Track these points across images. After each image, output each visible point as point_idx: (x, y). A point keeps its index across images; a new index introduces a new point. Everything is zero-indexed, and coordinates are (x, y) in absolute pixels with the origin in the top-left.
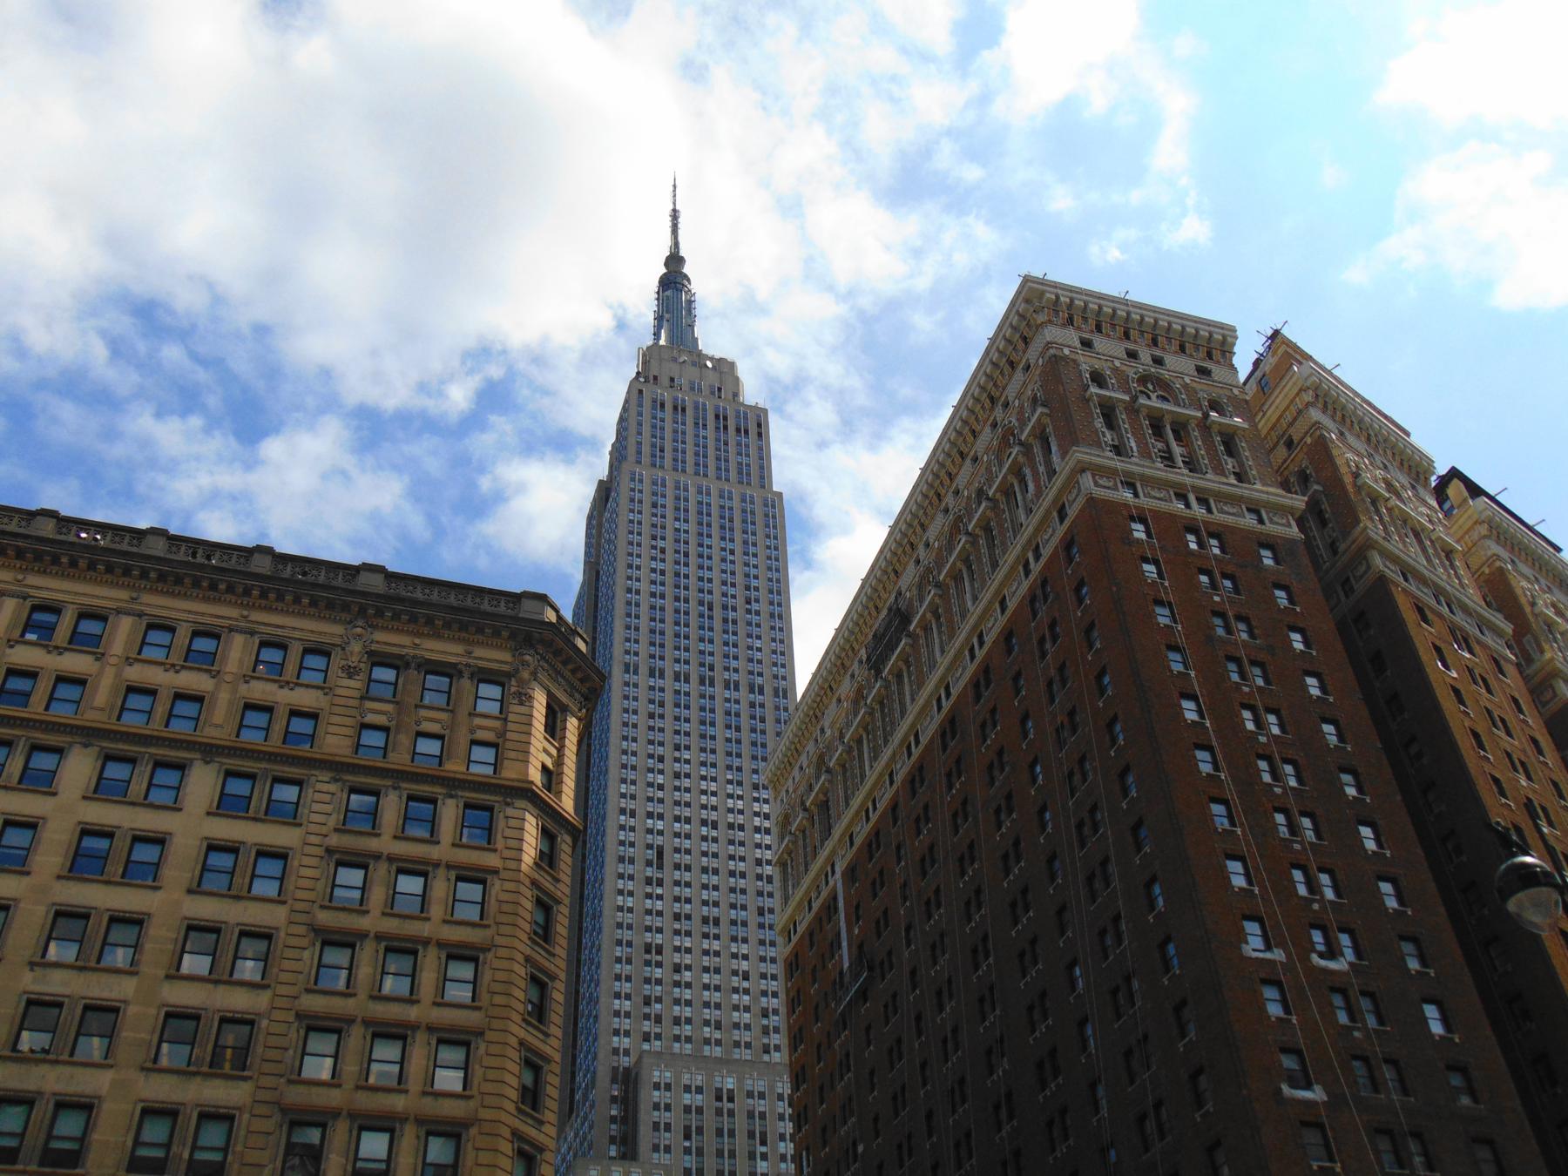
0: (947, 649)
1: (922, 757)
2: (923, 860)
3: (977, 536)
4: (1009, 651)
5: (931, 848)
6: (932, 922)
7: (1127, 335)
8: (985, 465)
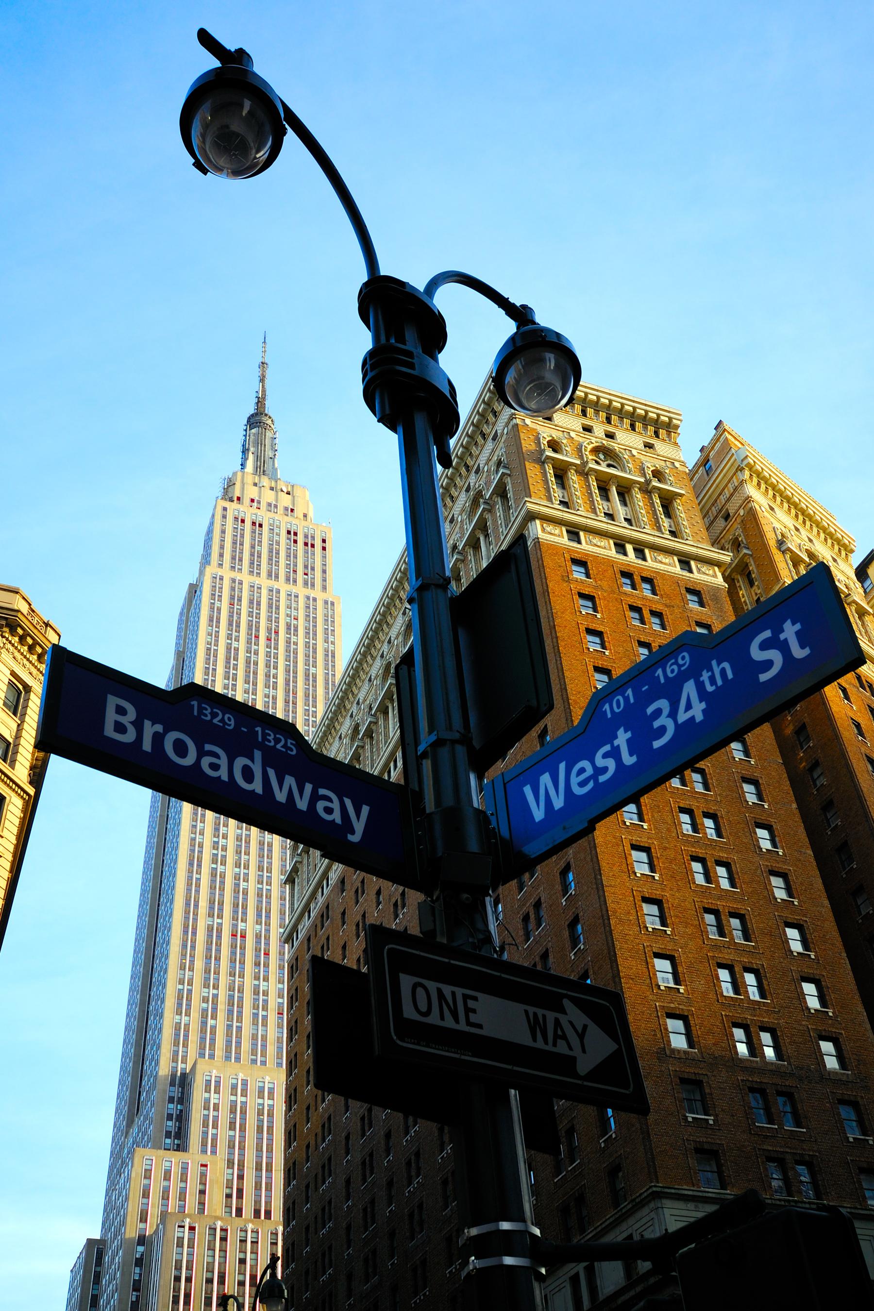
7: (584, 413)
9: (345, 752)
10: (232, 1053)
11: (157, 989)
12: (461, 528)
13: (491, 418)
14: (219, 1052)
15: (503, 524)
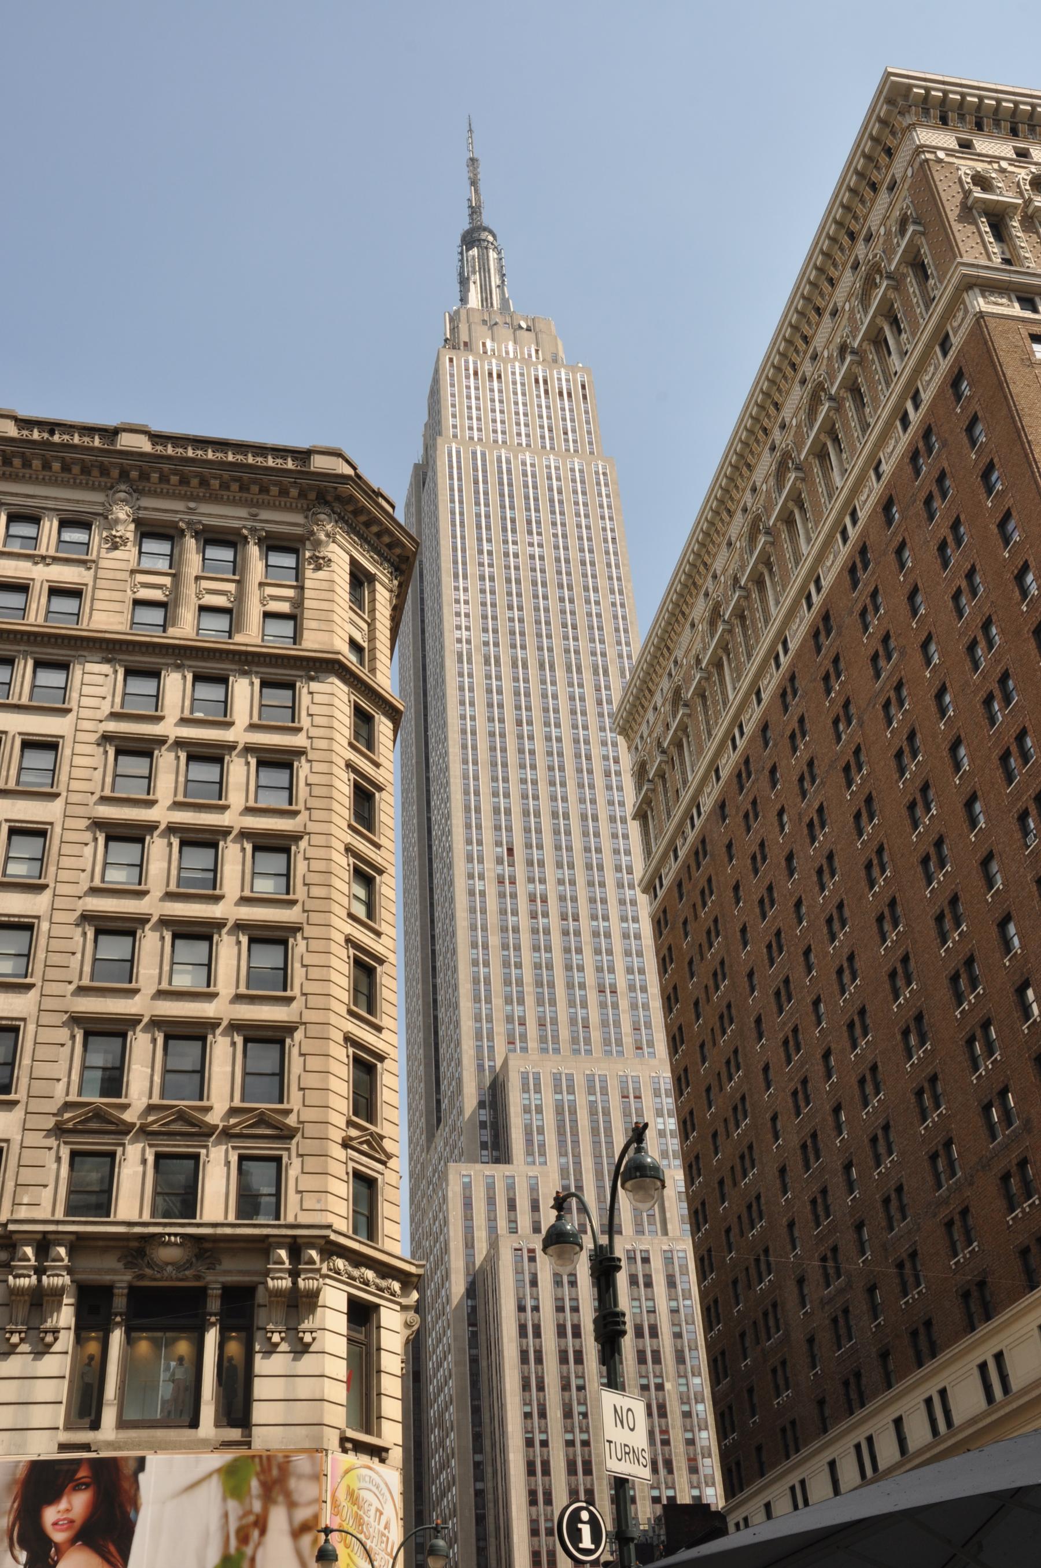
0: (813, 536)
1: (793, 664)
2: (801, 779)
3: (843, 399)
4: (889, 521)
5: (811, 764)
6: (816, 844)
8: (846, 316)
9: (703, 640)
10: (548, 1042)
11: (445, 975)
12: (852, 319)
13: (883, 159)
14: (533, 1044)
15: (921, 302)
